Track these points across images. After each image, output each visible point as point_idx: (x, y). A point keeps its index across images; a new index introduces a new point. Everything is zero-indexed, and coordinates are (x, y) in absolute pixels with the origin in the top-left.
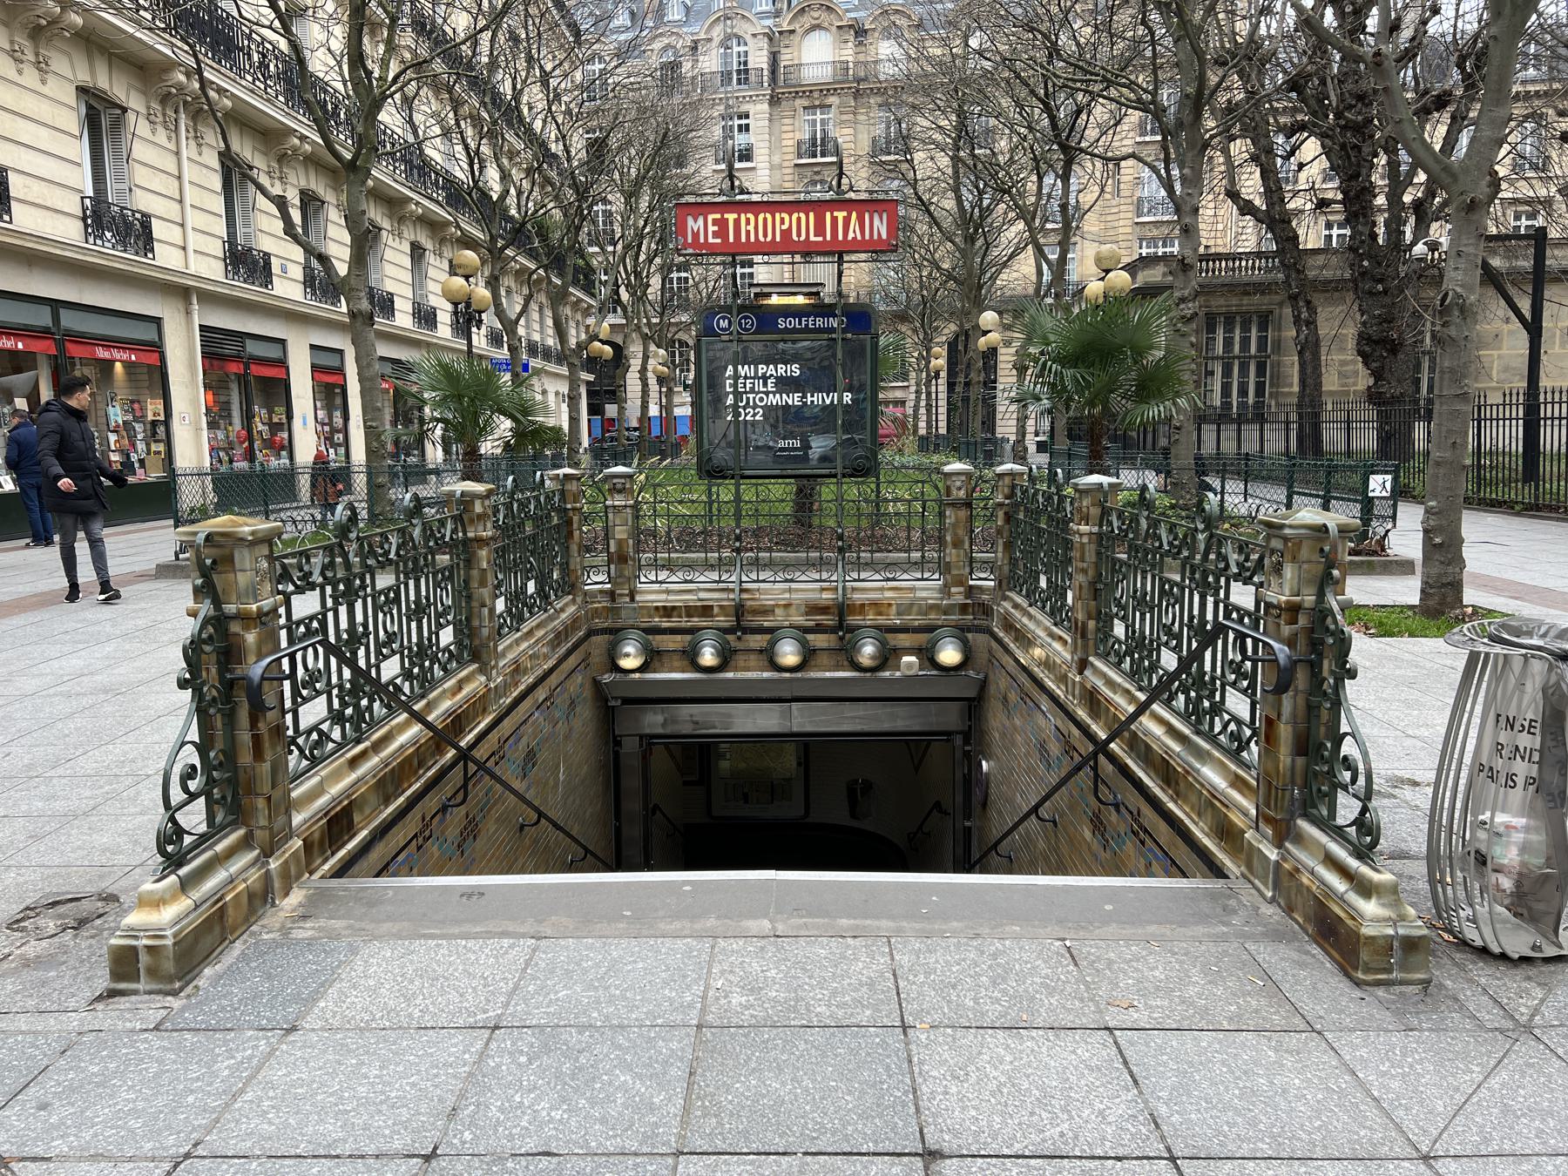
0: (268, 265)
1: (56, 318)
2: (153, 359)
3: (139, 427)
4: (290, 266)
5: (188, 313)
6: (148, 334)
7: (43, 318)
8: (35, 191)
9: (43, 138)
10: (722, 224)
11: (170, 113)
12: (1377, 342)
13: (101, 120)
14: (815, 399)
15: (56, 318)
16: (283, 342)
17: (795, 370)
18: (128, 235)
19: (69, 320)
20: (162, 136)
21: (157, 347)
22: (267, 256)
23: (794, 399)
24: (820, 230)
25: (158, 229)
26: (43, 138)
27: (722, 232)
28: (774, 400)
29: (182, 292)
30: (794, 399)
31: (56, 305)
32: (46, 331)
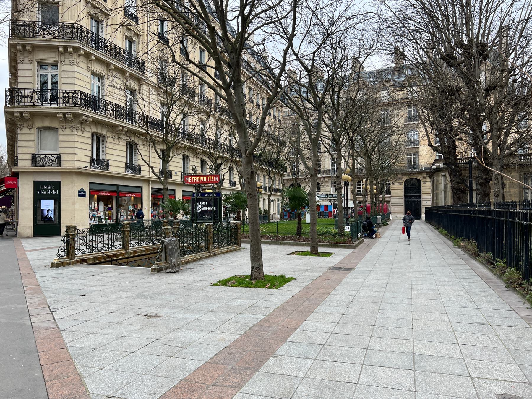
0: (171, 173)
1: (118, 188)
2: (139, 196)
3: (136, 210)
4: (178, 173)
5: (149, 185)
6: (139, 190)
7: (115, 188)
8: (116, 164)
9: (118, 153)
10: (191, 179)
11: (148, 143)
12: (457, 189)
13: (132, 147)
14: (209, 208)
15: (118, 188)
16: (175, 190)
17: (206, 203)
18: (135, 170)
19: (120, 189)
20: (146, 148)
21: (141, 193)
22: (171, 171)
23: (206, 209)
24: (207, 180)
25: (142, 168)
26: (118, 153)
27: (191, 180)
28: (203, 209)
29: (147, 181)
30: (206, 209)
31: (118, 186)
32: (115, 191)
